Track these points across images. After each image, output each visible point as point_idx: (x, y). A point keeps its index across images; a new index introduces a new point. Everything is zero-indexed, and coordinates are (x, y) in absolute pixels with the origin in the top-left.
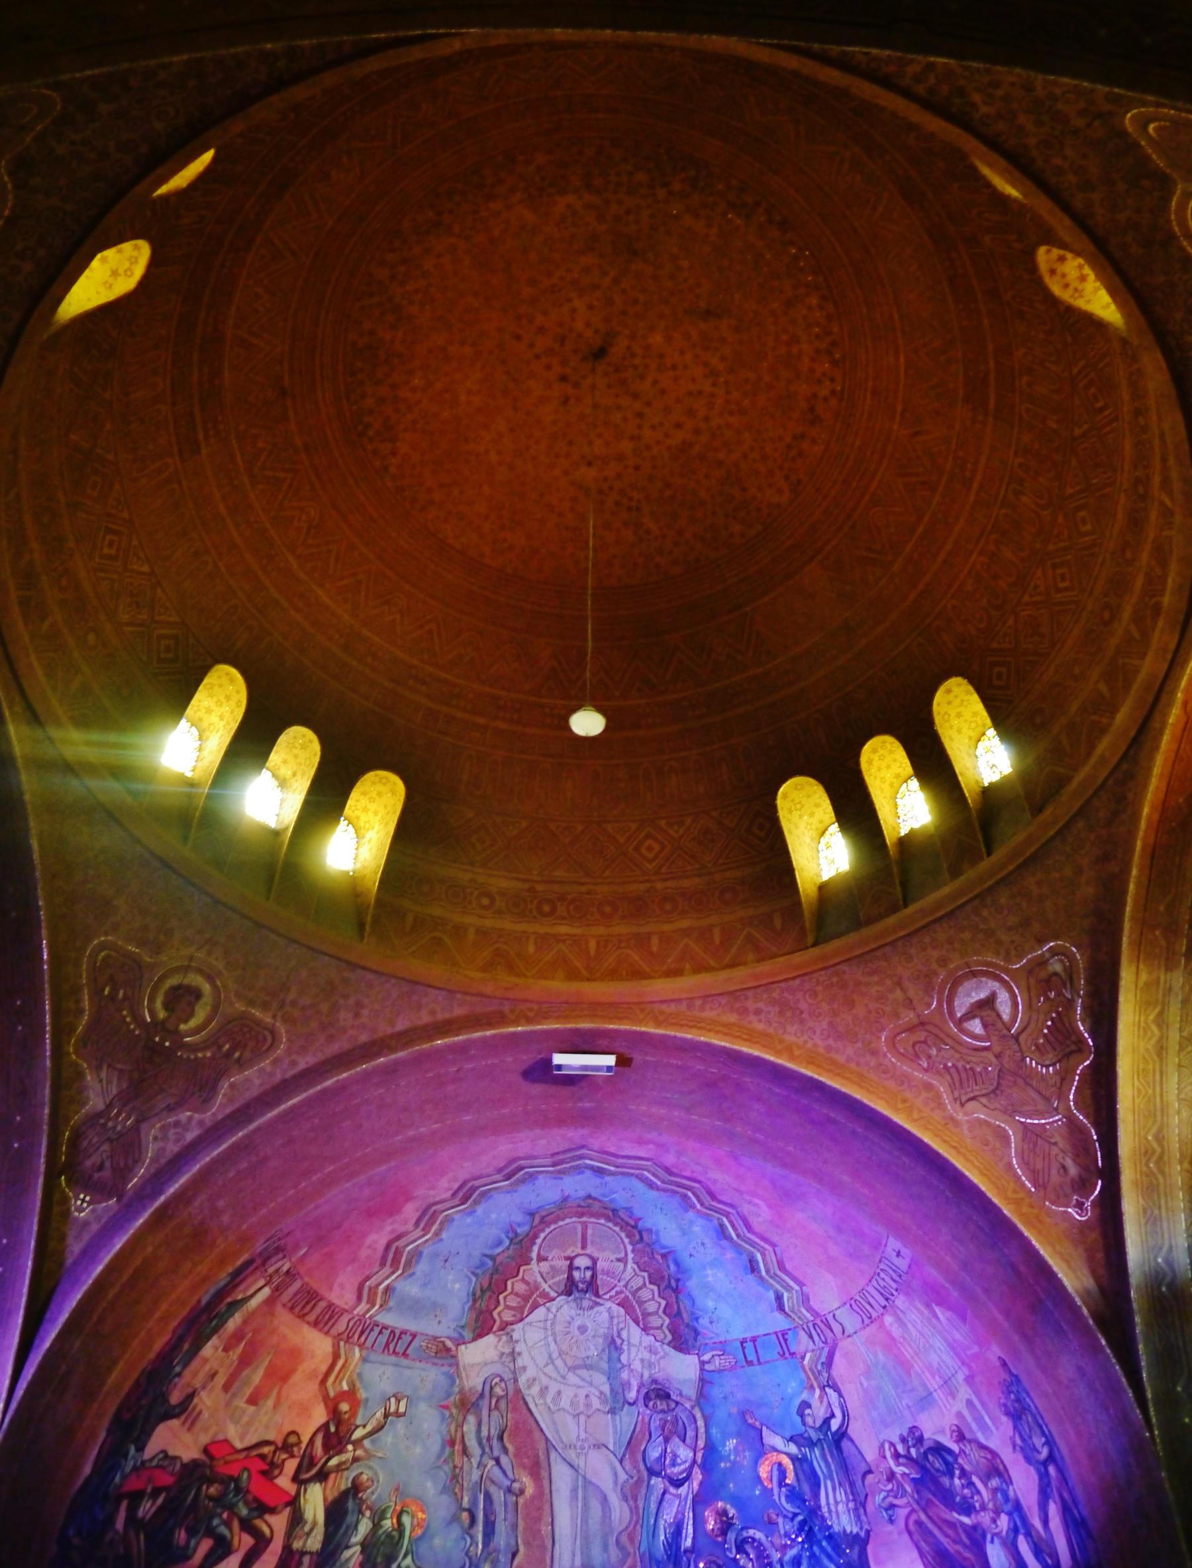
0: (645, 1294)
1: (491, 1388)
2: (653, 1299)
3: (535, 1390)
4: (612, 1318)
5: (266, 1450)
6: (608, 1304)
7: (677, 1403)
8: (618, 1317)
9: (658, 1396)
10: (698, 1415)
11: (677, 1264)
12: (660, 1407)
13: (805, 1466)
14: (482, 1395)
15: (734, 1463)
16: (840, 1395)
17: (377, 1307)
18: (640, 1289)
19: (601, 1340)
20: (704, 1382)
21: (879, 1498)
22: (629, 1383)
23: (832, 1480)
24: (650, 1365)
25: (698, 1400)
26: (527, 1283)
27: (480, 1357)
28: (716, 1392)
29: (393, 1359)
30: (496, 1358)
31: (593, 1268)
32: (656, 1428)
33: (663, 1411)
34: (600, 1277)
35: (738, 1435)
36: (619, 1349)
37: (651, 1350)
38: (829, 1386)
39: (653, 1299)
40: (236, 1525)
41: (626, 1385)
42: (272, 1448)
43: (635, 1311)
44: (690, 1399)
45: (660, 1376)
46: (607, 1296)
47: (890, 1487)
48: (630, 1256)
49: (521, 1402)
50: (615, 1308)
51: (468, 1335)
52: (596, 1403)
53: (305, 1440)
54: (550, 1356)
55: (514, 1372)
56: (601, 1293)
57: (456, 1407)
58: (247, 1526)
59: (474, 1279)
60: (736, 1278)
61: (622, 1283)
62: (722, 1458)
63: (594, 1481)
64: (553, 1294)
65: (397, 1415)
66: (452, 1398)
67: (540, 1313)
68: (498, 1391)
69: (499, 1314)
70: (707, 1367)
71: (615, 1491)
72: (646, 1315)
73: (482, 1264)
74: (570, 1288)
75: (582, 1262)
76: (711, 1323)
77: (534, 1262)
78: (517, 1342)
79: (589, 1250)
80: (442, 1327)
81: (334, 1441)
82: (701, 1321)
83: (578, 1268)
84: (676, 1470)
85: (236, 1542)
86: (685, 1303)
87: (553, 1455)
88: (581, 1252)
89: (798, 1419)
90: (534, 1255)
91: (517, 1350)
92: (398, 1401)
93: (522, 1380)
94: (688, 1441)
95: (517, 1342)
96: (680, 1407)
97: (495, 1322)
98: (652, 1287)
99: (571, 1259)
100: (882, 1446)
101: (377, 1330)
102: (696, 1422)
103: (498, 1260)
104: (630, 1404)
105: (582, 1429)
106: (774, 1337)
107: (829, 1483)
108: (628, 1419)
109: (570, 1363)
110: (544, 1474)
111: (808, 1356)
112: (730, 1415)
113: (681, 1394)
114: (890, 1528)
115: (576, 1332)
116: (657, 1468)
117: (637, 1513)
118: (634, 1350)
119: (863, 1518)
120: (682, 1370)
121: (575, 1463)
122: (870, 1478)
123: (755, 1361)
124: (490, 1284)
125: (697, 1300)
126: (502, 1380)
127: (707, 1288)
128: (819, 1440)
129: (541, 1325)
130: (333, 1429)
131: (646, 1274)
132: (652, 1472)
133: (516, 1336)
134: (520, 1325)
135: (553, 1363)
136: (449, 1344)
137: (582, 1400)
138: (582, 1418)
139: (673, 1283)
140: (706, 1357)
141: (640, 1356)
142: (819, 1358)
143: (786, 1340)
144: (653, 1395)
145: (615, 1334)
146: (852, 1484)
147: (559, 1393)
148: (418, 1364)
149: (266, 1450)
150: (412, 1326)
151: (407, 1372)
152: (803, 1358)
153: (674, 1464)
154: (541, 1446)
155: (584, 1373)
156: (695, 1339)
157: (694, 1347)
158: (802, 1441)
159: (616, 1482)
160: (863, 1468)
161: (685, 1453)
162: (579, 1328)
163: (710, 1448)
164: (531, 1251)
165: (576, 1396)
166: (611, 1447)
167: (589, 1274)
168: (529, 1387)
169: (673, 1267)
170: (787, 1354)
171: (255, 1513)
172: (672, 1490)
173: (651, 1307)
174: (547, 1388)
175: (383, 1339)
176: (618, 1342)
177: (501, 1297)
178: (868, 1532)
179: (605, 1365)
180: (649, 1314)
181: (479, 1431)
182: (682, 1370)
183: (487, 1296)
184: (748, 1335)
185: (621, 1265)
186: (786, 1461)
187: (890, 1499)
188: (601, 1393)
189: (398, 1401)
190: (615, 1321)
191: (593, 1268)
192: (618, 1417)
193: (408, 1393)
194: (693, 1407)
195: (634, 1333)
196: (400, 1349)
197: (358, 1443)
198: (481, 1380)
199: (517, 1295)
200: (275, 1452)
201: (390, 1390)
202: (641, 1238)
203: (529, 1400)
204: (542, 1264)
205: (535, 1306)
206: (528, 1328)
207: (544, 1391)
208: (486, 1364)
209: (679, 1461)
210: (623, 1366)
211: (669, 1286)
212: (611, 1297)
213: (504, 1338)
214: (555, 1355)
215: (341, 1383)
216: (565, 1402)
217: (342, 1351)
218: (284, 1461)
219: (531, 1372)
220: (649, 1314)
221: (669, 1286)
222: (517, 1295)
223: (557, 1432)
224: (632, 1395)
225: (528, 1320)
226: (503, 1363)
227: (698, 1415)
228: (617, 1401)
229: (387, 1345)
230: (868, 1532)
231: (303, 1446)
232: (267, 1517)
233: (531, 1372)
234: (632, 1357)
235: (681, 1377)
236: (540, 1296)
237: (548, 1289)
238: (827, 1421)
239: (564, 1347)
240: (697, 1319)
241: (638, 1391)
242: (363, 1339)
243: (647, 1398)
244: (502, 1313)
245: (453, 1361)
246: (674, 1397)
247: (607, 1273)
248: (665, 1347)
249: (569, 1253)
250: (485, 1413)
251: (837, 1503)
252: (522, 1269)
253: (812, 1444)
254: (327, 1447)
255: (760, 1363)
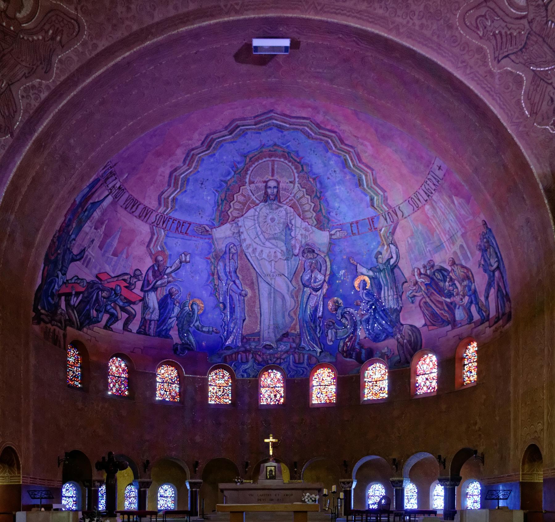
0: (304, 201)
1: (230, 249)
2: (308, 203)
3: (250, 250)
4: (287, 214)
5: (126, 277)
6: (285, 207)
7: (318, 254)
8: (290, 213)
9: (309, 252)
10: (328, 260)
11: (321, 183)
12: (309, 257)
13: (376, 280)
14: (225, 253)
15: (343, 281)
16: (397, 248)
17: (169, 209)
18: (301, 198)
19: (281, 225)
20: (332, 243)
21: (408, 293)
22: (295, 246)
23: (388, 287)
24: (306, 237)
25: (327, 253)
26: (245, 196)
27: (223, 233)
28: (337, 249)
29: (181, 235)
30: (231, 235)
31: (277, 187)
32: (307, 266)
33: (311, 258)
34: (281, 192)
35: (346, 268)
36: (290, 229)
37: (306, 230)
38: (392, 243)
39: (308, 203)
40: (118, 308)
41: (294, 247)
42: (129, 276)
43: (298, 210)
44: (324, 252)
45: (310, 242)
46: (285, 203)
47: (414, 288)
48: (297, 180)
49: (244, 256)
50: (289, 208)
51: (216, 223)
52: (279, 255)
53: (144, 273)
54: (257, 234)
55: (240, 242)
56: (281, 201)
57: (214, 258)
58: (123, 309)
59: (217, 194)
60: (351, 190)
61: (292, 195)
62: (337, 279)
63: (279, 290)
64: (257, 202)
65: (186, 262)
66: (211, 254)
67: (251, 212)
68: (233, 250)
69: (231, 213)
70: (333, 237)
71: (288, 294)
72: (304, 211)
73: (221, 186)
74: (266, 198)
75: (272, 184)
76: (336, 215)
77: (247, 184)
78: (240, 227)
79: (275, 178)
80: (204, 220)
81: (158, 274)
82: (331, 214)
83: (270, 187)
84: (316, 284)
85: (120, 315)
86: (323, 206)
87: (260, 279)
88: (271, 178)
89: (375, 260)
90: (247, 180)
91: (241, 231)
92: (186, 256)
93: (244, 245)
94: (322, 272)
95: (240, 227)
96: (319, 256)
97: (229, 216)
98: (307, 196)
99: (266, 182)
100: (414, 270)
101: (171, 221)
102: (326, 263)
103: (229, 183)
104: (295, 256)
105: (273, 267)
106: (367, 221)
107: (386, 288)
108: (294, 262)
109: (266, 237)
110: (256, 287)
111: (383, 229)
112: (342, 259)
113: (320, 251)
114: (412, 305)
115: (270, 221)
116: (307, 284)
117: (298, 303)
118: (298, 230)
119: (400, 302)
120: (321, 238)
121: (270, 282)
122: (406, 284)
123: (357, 233)
124: (226, 196)
125: (330, 203)
126: (235, 245)
127: (336, 196)
128: (384, 269)
129: (252, 218)
130: (156, 268)
131: (304, 190)
132: (305, 286)
133: (240, 224)
134: (242, 218)
135: (258, 237)
136: (208, 228)
137: (273, 254)
138: (273, 263)
139: (318, 195)
140: (333, 232)
141: (300, 233)
142: (389, 230)
143: (373, 222)
144: (306, 251)
145: (289, 221)
146: (397, 288)
147: (262, 251)
148: (193, 238)
149: (126, 277)
150: (189, 219)
151: (188, 242)
152: (381, 230)
153: (315, 282)
154: (254, 275)
155: (273, 241)
156: (328, 223)
157: (327, 227)
158: (376, 270)
159: (288, 291)
160: (404, 280)
161: (320, 277)
162: (271, 219)
163: (333, 275)
164: (245, 178)
165: (270, 252)
166: (286, 275)
167: (275, 190)
168: (248, 249)
169: (318, 185)
170: (373, 229)
171: (126, 304)
172: (314, 293)
173: (307, 207)
174: (256, 249)
175: (175, 225)
176: (290, 226)
177: (231, 204)
178: (401, 307)
179: (284, 238)
180: (306, 211)
181: (225, 269)
182: (321, 238)
183: (225, 202)
184: (354, 220)
185: (292, 185)
186: (367, 279)
187: (414, 293)
188: (282, 251)
189: (186, 256)
190: (289, 215)
191: (277, 187)
192: (289, 262)
193: (190, 252)
194: (325, 256)
195: (299, 221)
196: (184, 231)
197: (167, 275)
198: (224, 245)
199: (239, 202)
200: (130, 278)
201: (181, 251)
202: (303, 170)
203: (248, 254)
204: (252, 185)
205: (249, 208)
206: (245, 220)
207: (254, 250)
208: (226, 238)
209: (317, 280)
210: (293, 238)
211: (316, 196)
212: (287, 203)
213: (234, 225)
214: (259, 233)
215: (157, 247)
216: (264, 256)
217: (155, 231)
218: (135, 282)
219: (248, 242)
220: (306, 211)
221: (316, 196)
222: (239, 202)
223: (261, 269)
224: (296, 252)
225: (245, 216)
226: (234, 237)
227: (328, 260)
228: (289, 254)
229: (177, 228)
230: (401, 307)
231: (144, 276)
232: (132, 306)
233: (248, 242)
234: (297, 233)
235: (320, 242)
236: (251, 203)
237: (255, 199)
238: (388, 260)
239: (264, 229)
240: (329, 213)
241: (299, 250)
242: (164, 225)
243: (303, 252)
244: (233, 213)
245: (210, 236)
246: (316, 252)
247: (285, 190)
248: (313, 228)
249: (265, 179)
250: (227, 261)
251: (389, 296)
252: (241, 188)
253: (380, 271)
254: (155, 276)
255: (359, 234)
